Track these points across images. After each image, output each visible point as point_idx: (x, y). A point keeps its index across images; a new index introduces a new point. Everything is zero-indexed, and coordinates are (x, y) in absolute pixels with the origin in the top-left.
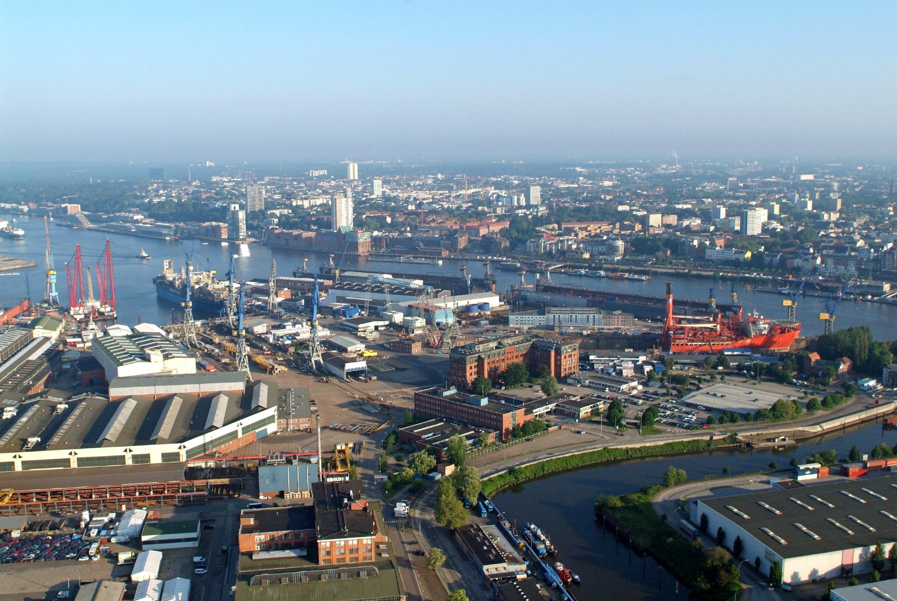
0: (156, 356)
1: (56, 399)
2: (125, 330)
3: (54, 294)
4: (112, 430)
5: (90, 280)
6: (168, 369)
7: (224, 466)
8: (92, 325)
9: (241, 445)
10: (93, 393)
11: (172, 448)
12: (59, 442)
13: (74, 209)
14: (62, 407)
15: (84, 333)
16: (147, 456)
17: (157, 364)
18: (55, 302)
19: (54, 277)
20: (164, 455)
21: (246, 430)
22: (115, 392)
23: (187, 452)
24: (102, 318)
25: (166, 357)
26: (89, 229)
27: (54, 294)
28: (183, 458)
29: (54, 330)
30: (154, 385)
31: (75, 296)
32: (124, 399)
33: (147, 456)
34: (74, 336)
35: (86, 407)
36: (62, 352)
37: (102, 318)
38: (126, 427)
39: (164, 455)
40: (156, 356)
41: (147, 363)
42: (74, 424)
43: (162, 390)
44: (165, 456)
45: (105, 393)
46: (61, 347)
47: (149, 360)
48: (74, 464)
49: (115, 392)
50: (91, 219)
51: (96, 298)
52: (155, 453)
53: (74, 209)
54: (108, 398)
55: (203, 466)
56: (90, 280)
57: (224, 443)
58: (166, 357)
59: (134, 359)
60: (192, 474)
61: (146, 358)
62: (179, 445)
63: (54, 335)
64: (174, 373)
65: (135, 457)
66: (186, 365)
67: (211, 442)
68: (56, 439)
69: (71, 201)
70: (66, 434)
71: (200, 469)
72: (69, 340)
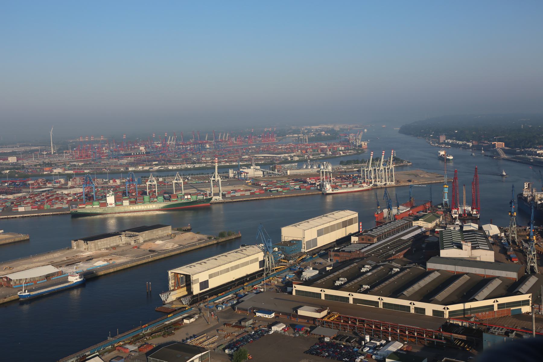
0: (467, 246)
1: (396, 265)
2: (474, 226)
3: (446, 199)
4: (410, 289)
5: (464, 193)
6: (473, 256)
7: (474, 327)
8: (458, 222)
9: (496, 316)
10: (419, 264)
11: (440, 308)
12: (377, 291)
13: (500, 145)
14: (397, 270)
15: (448, 226)
16: (424, 310)
17: (466, 252)
18: (446, 204)
19: (447, 189)
20: (434, 311)
21: (500, 306)
22: (430, 266)
23: (449, 312)
24: (471, 217)
25: (473, 248)
26: (504, 159)
27: (446, 199)
28: (447, 316)
29: (431, 222)
30: (455, 265)
31: (455, 203)
32: (432, 271)
33: (424, 310)
34: (442, 227)
35: (409, 272)
36: (428, 236)
37: (471, 217)
38: (422, 289)
39: (434, 311)
40: (467, 246)
41: (460, 250)
42: (394, 281)
43: (459, 269)
44: (434, 311)
45: (425, 266)
46: (428, 233)
47: (462, 249)
48: (381, 306)
49: (430, 266)
50: (506, 152)
51: (468, 204)
52: (429, 308)
53: (500, 145)
54: (426, 268)
55: (460, 324)
56: (464, 193)
57: (481, 312)
58: (473, 248)
59: (453, 247)
60: (448, 327)
61: (460, 247)
62: (444, 306)
63: (430, 226)
64: (478, 259)
65: (416, 309)
66: (487, 255)
67: (470, 309)
68: (376, 289)
69: (499, 140)
70: (385, 286)
71: (457, 325)
72: (436, 230)
